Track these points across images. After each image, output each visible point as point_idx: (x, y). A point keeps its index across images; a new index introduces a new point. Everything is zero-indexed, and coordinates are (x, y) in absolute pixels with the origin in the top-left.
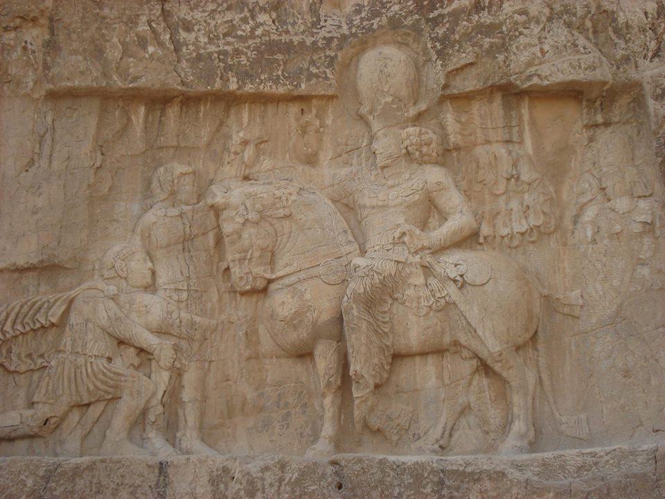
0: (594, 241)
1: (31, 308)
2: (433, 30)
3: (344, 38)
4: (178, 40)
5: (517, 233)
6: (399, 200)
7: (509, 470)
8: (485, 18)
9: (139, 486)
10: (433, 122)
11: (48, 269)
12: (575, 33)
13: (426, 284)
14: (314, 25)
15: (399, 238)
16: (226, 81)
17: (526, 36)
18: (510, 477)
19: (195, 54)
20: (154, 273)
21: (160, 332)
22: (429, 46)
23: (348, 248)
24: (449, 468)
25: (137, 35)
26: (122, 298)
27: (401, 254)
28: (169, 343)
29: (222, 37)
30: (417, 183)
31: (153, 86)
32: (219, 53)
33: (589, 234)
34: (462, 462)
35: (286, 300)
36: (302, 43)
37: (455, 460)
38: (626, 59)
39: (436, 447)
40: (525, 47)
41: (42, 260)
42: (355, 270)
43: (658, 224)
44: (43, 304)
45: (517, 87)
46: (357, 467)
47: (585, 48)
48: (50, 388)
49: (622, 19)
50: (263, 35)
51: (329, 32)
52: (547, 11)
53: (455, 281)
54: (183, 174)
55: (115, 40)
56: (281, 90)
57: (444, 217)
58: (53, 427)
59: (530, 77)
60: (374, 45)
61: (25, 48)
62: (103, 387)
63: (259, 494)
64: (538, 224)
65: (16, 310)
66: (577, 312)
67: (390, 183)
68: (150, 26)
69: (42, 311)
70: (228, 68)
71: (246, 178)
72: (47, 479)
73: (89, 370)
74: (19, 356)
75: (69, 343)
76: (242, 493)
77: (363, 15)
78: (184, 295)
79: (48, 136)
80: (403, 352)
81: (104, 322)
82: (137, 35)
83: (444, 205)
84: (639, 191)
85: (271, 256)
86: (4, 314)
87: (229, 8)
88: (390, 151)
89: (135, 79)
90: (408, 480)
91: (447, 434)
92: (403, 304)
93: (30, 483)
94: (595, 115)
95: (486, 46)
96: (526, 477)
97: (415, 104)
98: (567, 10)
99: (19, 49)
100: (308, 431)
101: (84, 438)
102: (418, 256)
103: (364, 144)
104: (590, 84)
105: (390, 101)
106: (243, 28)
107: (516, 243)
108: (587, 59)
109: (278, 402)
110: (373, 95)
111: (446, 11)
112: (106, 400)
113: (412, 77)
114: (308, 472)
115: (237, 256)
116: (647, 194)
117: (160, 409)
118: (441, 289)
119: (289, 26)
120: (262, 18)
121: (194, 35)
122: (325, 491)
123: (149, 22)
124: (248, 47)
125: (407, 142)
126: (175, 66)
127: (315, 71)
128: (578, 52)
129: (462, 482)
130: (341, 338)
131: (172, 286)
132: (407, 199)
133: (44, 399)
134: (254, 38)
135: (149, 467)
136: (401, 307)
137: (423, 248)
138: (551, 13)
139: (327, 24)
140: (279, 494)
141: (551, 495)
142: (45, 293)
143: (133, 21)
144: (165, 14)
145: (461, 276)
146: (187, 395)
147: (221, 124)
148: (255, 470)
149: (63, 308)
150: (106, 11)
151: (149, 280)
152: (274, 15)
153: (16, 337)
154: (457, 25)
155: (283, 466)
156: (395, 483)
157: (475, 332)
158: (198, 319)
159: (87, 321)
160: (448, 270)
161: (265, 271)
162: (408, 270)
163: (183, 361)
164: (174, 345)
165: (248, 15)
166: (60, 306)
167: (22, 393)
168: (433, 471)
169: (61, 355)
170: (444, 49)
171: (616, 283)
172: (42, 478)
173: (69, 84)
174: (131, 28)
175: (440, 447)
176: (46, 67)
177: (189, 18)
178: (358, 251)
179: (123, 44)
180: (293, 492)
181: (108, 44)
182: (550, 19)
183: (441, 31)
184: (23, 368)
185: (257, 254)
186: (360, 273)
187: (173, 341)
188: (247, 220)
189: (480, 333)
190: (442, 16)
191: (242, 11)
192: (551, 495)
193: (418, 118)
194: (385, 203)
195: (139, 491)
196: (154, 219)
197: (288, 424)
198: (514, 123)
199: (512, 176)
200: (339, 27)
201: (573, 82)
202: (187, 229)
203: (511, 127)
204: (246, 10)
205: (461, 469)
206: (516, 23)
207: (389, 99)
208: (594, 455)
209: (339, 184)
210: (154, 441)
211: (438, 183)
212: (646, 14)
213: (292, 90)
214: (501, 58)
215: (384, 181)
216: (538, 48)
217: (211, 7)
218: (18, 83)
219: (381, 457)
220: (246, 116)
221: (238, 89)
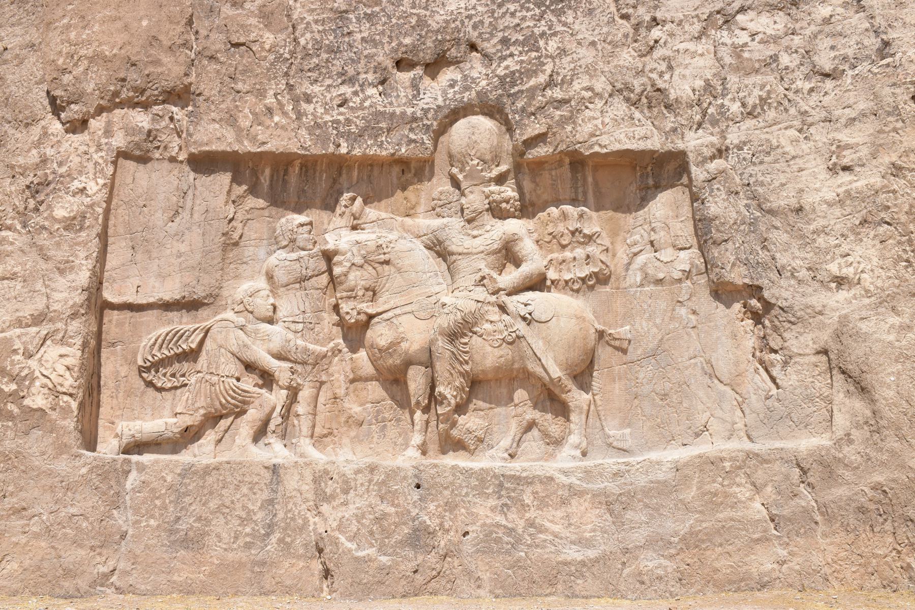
0: (642, 285)
1: (175, 336)
2: (513, 104)
3: (439, 107)
4: (299, 112)
5: (579, 278)
6: (482, 248)
7: (557, 475)
8: (557, 93)
9: (257, 483)
11: (191, 305)
12: (633, 108)
14: (414, 96)
15: (480, 281)
16: (339, 146)
17: (591, 110)
18: (557, 481)
19: (312, 123)
20: (275, 308)
21: (279, 357)
22: (510, 117)
23: (437, 289)
24: (508, 473)
25: (265, 105)
26: (250, 327)
27: (481, 293)
28: (286, 365)
29: (335, 107)
31: (277, 149)
32: (333, 122)
33: (638, 279)
34: (519, 468)
35: (383, 332)
36: (404, 113)
37: (516, 466)
38: (674, 130)
39: (506, 455)
40: (589, 120)
41: (184, 297)
43: (694, 271)
44: (185, 332)
45: (581, 153)
46: (433, 471)
47: (639, 121)
48: (190, 402)
49: (672, 96)
50: (371, 106)
51: (427, 104)
52: (609, 88)
53: (524, 319)
54: (302, 225)
55: (247, 111)
56: (384, 153)
57: (517, 263)
58: (192, 434)
59: (591, 147)
60: (465, 116)
61: (172, 119)
62: (233, 401)
63: (352, 491)
64: (596, 270)
65: (162, 338)
66: (625, 345)
67: (475, 233)
68: (276, 98)
69: (184, 338)
70: (340, 135)
71: (354, 228)
72: (182, 475)
73: (222, 388)
74: (164, 375)
75: (205, 365)
76: (338, 490)
77: (457, 88)
78: (300, 327)
79: (190, 193)
80: (481, 376)
81: (235, 349)
82: (265, 105)
84: (681, 243)
85: (373, 292)
86: (153, 340)
87: (343, 83)
89: (264, 143)
90: (474, 482)
91: (515, 445)
92: (481, 336)
93: (169, 479)
94: (647, 178)
95: (557, 118)
96: (570, 481)
97: (497, 166)
98: (628, 88)
99: (167, 118)
100: (400, 440)
101: (220, 441)
104: (643, 152)
106: (354, 100)
107: (576, 287)
108: (640, 131)
109: (376, 417)
111: (524, 88)
112: (235, 413)
113: (495, 143)
114: (393, 473)
115: (345, 294)
116: (688, 246)
117: (280, 420)
119: (393, 99)
120: (371, 91)
121: (312, 105)
122: (406, 490)
123: (275, 95)
124: (357, 117)
126: (296, 133)
127: (412, 136)
128: (634, 125)
129: (518, 484)
130: (429, 364)
131: (291, 319)
133: (184, 411)
134: (363, 110)
135: (266, 468)
136: (480, 339)
137: (500, 290)
138: (612, 90)
139: (425, 96)
140: (368, 492)
141: (589, 496)
142: (187, 324)
143: (261, 94)
144: (290, 87)
145: (530, 314)
146: (301, 408)
147: (335, 181)
148: (349, 472)
149: (202, 335)
150: (240, 86)
151: (271, 314)
152: (381, 88)
153: (162, 360)
154: (534, 99)
155: (372, 469)
156: (464, 485)
157: (540, 360)
158: (311, 347)
159: (221, 347)
161: (367, 307)
162: (486, 308)
163: (299, 381)
164: (292, 368)
165: (359, 89)
166: (198, 334)
167: (168, 404)
168: (495, 476)
169: (199, 375)
170: (521, 120)
171: (658, 321)
172: (179, 475)
173: (207, 149)
174: (260, 100)
175: (510, 455)
176: (190, 135)
177: (309, 92)
179: (255, 114)
180: (380, 490)
181: (241, 115)
182: (611, 95)
183: (520, 104)
184: (169, 385)
185: (360, 293)
186: (446, 311)
187: (290, 365)
188: (353, 264)
189: (543, 361)
190: (522, 92)
191: (354, 84)
192: (589, 496)
193: (500, 180)
194: (470, 251)
195: (256, 487)
196: (277, 262)
197: (385, 435)
198: (579, 184)
199: (577, 229)
200: (436, 99)
201: (628, 152)
202: (304, 271)
203: (576, 189)
204: (357, 85)
205: (518, 474)
206: (583, 98)
207: (476, 162)
208: (627, 464)
210: (274, 446)
212: (694, 90)
213: (393, 155)
214: (569, 128)
215: (470, 232)
216: (600, 121)
217: (328, 82)
218: (166, 148)
219: (454, 463)
220: (355, 173)
221: (347, 153)
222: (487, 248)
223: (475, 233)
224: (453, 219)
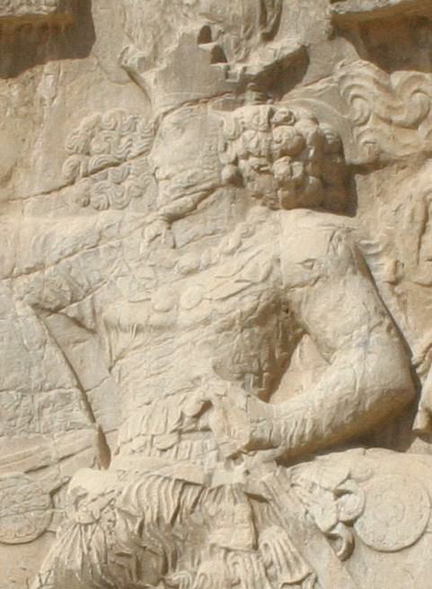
10: (318, 86)
13: (256, 547)
15: (198, 416)
23: (68, 442)
30: (255, 261)
42: (76, 503)
53: (332, 538)
67: (187, 260)
83: (322, 325)
88: (190, 173)
97: (268, 37)
102: (239, 469)
103: (135, 151)
105: (197, 33)
110: (157, 16)
118: (291, 561)
125: (236, 148)
132: (223, 307)
137: (255, 445)
160: (315, 510)
178: (94, 451)
186: (81, 516)
207: (196, 27)
209: (57, 262)
211: (309, 263)
215: (169, 255)
222: (223, 307)
223: (187, 260)
224: (129, 213)
